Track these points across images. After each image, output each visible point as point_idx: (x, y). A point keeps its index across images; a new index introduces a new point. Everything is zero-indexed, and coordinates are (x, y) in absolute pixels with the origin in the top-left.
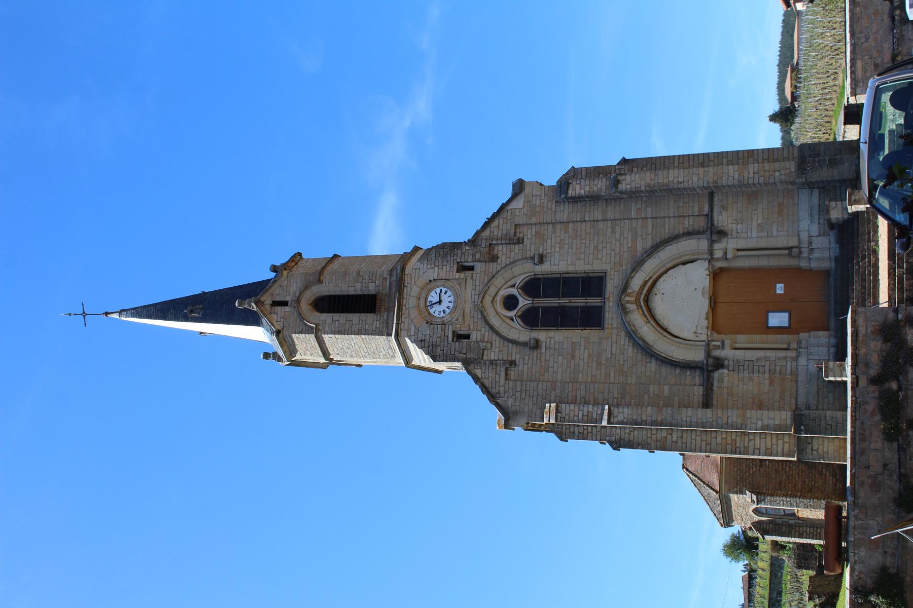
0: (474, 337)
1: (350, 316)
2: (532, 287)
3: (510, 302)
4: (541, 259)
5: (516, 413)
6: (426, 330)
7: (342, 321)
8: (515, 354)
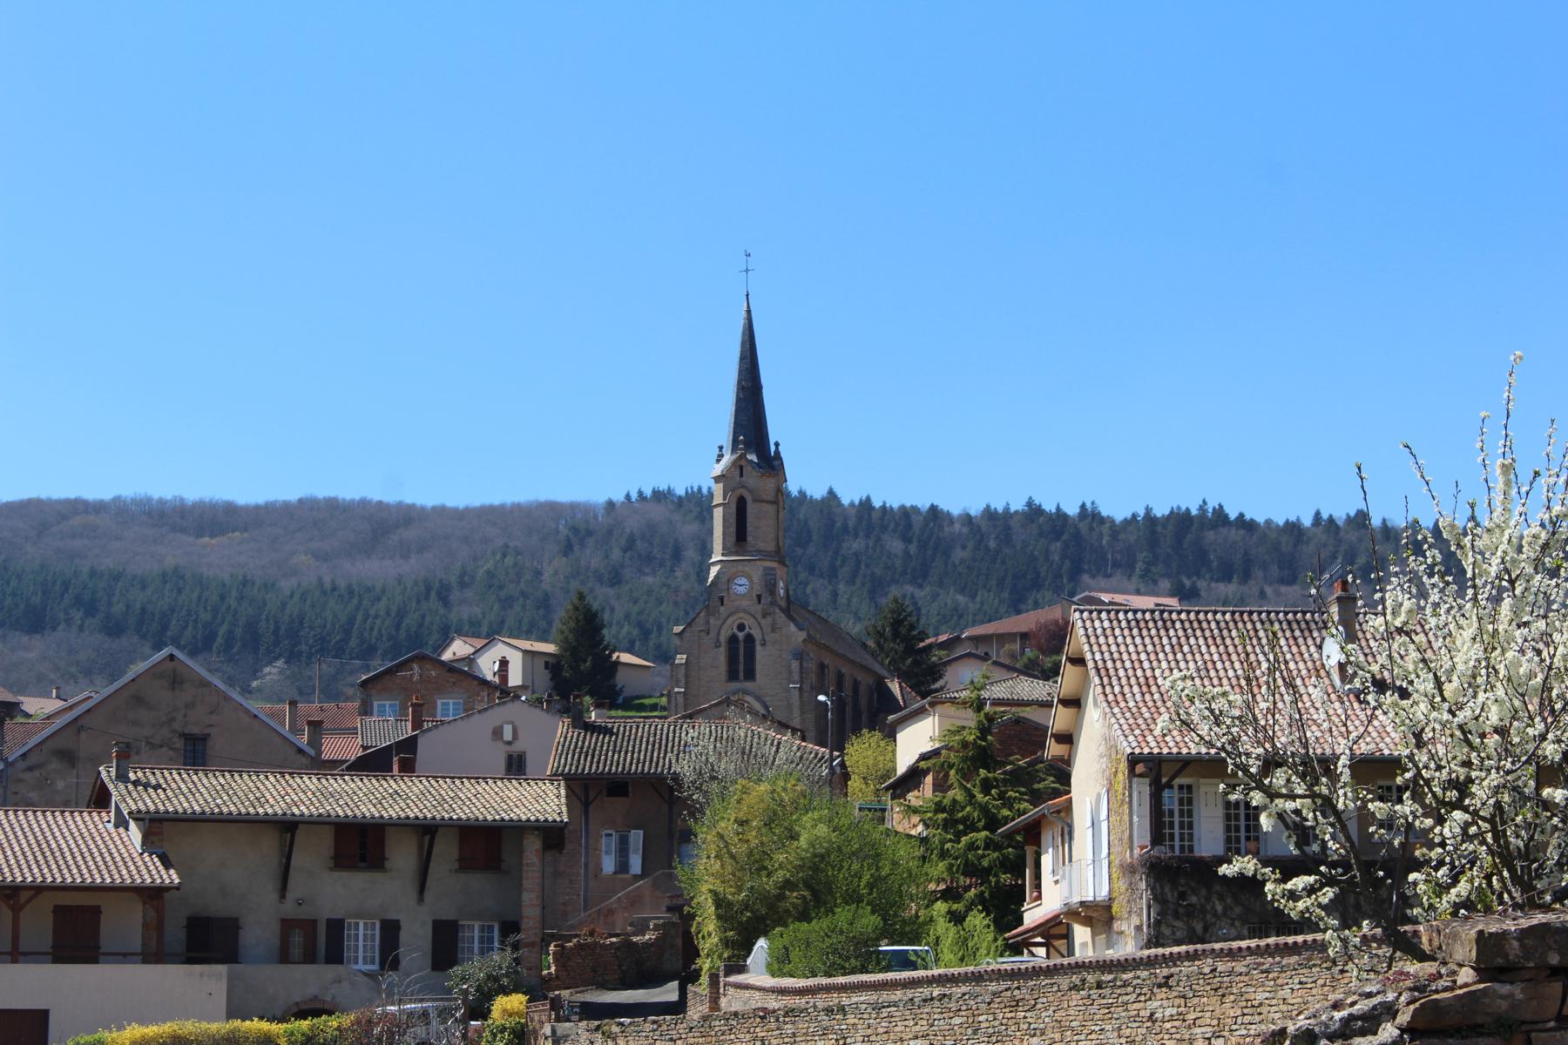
0: (722, 608)
1: (734, 525)
2: (750, 639)
3: (741, 627)
4: (764, 644)
5: (682, 639)
6: (724, 579)
7: (731, 521)
8: (713, 634)
